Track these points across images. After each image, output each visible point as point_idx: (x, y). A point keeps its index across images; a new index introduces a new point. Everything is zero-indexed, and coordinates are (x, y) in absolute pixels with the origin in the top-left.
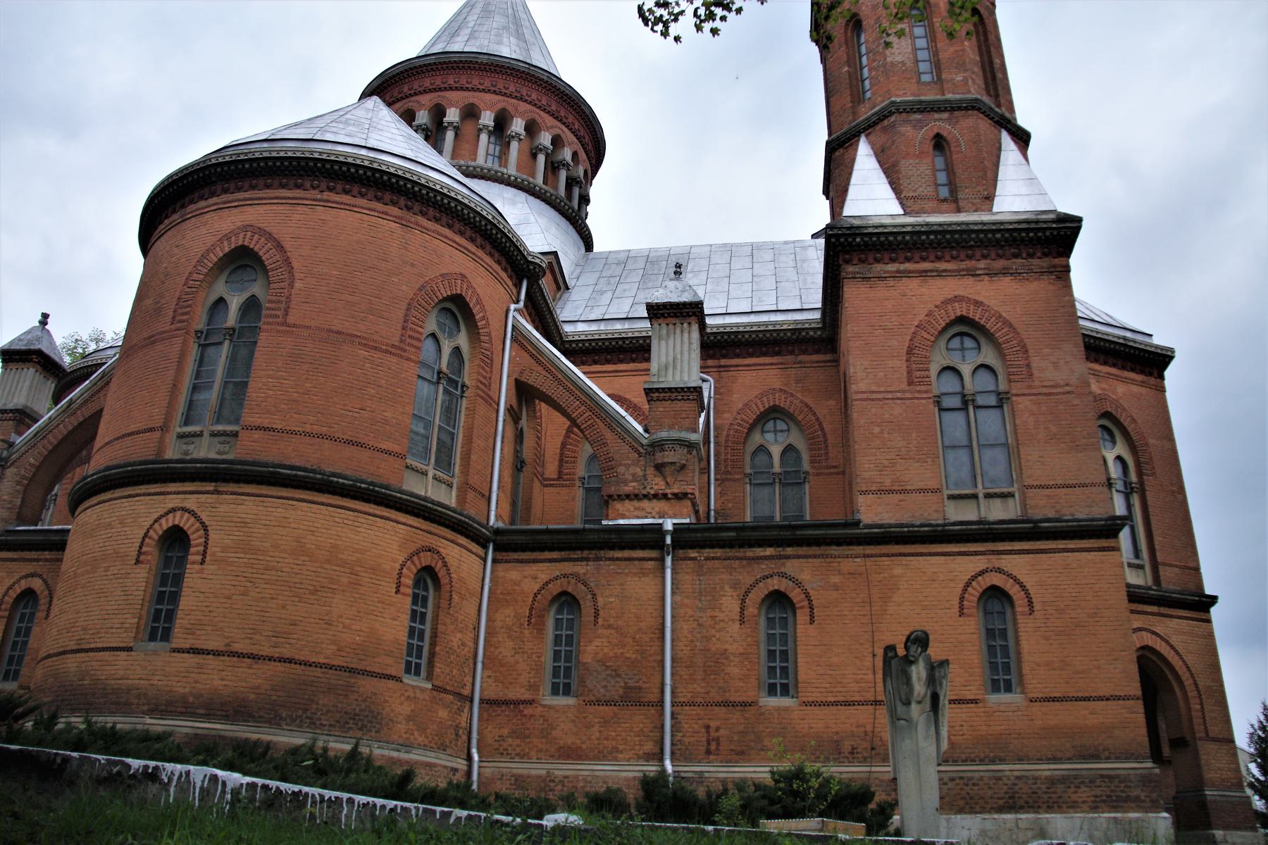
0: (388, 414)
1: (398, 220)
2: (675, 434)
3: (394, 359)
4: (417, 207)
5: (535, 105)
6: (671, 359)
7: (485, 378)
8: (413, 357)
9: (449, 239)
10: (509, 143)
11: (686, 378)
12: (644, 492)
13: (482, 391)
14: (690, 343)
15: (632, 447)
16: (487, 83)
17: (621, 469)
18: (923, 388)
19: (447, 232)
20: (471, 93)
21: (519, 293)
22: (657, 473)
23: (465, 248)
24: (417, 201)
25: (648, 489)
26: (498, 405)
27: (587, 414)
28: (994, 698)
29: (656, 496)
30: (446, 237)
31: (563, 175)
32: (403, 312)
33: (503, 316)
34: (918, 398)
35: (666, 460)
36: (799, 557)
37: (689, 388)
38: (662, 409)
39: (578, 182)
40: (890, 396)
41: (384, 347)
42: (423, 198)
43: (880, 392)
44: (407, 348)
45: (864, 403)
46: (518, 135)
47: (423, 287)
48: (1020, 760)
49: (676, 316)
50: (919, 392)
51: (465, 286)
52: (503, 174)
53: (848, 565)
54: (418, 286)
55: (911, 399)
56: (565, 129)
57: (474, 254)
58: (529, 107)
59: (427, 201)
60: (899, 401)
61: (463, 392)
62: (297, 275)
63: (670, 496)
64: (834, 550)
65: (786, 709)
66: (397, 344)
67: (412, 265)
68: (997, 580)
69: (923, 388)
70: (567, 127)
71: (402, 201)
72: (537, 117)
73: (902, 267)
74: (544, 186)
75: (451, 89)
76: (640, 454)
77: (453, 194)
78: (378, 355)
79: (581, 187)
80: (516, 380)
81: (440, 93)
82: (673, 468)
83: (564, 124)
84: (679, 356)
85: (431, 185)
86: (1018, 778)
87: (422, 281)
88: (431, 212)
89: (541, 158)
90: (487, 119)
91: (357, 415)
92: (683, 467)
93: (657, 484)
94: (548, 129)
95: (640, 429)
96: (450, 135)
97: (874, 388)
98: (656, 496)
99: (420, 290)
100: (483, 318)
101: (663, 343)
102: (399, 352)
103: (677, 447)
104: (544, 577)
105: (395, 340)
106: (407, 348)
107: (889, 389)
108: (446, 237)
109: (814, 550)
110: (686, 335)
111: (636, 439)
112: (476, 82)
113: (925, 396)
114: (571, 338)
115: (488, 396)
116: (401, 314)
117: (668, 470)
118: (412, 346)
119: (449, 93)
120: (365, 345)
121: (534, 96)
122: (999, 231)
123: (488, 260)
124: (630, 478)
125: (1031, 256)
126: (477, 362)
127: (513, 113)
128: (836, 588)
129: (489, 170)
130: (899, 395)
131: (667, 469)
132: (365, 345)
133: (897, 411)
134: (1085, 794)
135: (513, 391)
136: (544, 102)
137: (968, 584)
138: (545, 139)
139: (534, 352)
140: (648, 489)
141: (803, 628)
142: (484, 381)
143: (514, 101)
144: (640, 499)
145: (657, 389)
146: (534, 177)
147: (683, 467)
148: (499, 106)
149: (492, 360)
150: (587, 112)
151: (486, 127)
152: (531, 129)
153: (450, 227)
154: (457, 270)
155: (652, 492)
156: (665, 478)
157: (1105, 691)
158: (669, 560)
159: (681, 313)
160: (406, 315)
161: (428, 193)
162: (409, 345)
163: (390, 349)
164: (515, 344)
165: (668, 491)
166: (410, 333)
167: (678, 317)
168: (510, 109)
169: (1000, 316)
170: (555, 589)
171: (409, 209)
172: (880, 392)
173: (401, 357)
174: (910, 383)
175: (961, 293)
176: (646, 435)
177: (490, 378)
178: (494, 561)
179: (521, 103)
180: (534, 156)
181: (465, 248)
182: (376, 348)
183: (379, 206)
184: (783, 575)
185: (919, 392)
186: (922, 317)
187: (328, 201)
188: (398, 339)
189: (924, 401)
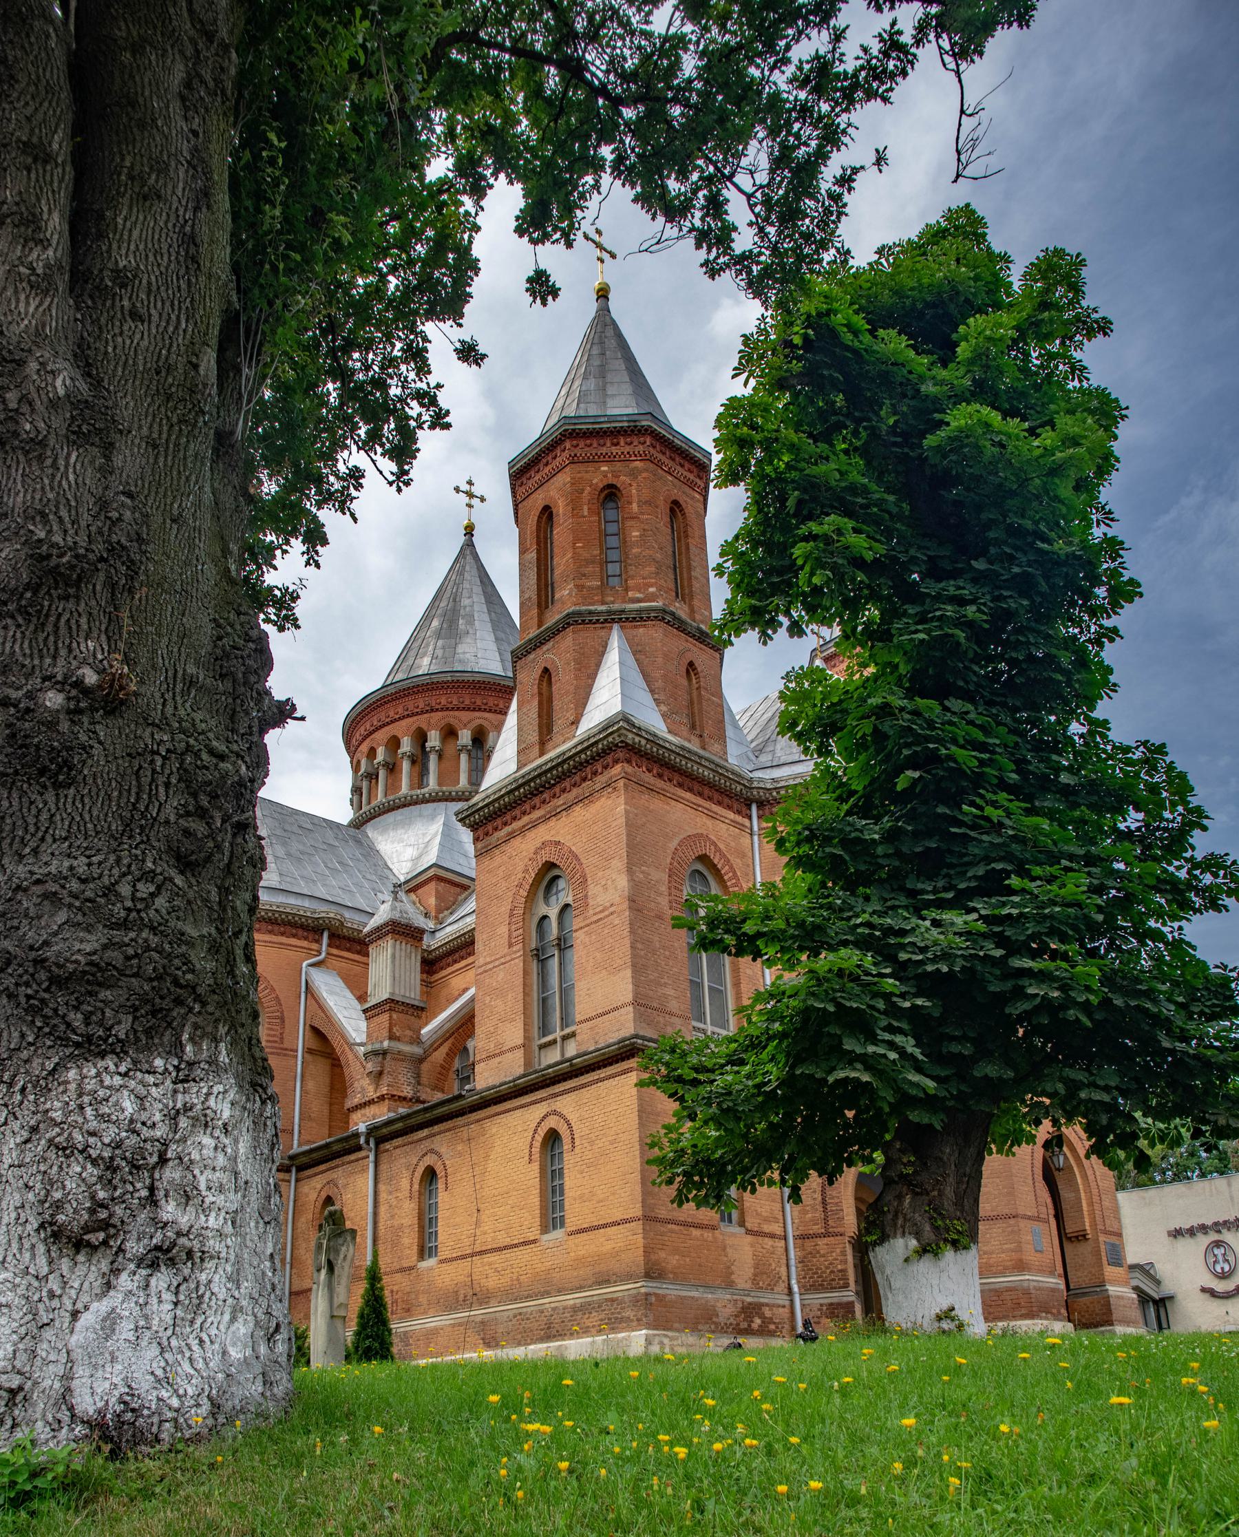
28: (546, 1237)
36: (440, 1133)
48: (560, 1291)
53: (464, 1132)
56: (487, 715)
64: (460, 1121)
65: (431, 1269)
68: (552, 1122)
72: (453, 721)
73: (508, 829)
86: (554, 1309)
89: (464, 758)
90: (406, 746)
92: (381, 1073)
93: (371, 1093)
96: (382, 773)
104: (319, 1186)
109: (450, 1124)
121: (443, 701)
122: (564, 761)
125: (595, 773)
128: (460, 1154)
133: (501, 975)
134: (595, 1318)
135: (309, 1033)
137: (535, 1131)
138: (465, 737)
141: (442, 1197)
147: (381, 1073)
148: (414, 728)
152: (450, 733)
157: (618, 1216)
158: (372, 1157)
169: (571, 851)
170: (324, 1195)
174: (510, 945)
175: (548, 838)
178: (297, 1180)
184: (432, 1151)
186: (520, 875)
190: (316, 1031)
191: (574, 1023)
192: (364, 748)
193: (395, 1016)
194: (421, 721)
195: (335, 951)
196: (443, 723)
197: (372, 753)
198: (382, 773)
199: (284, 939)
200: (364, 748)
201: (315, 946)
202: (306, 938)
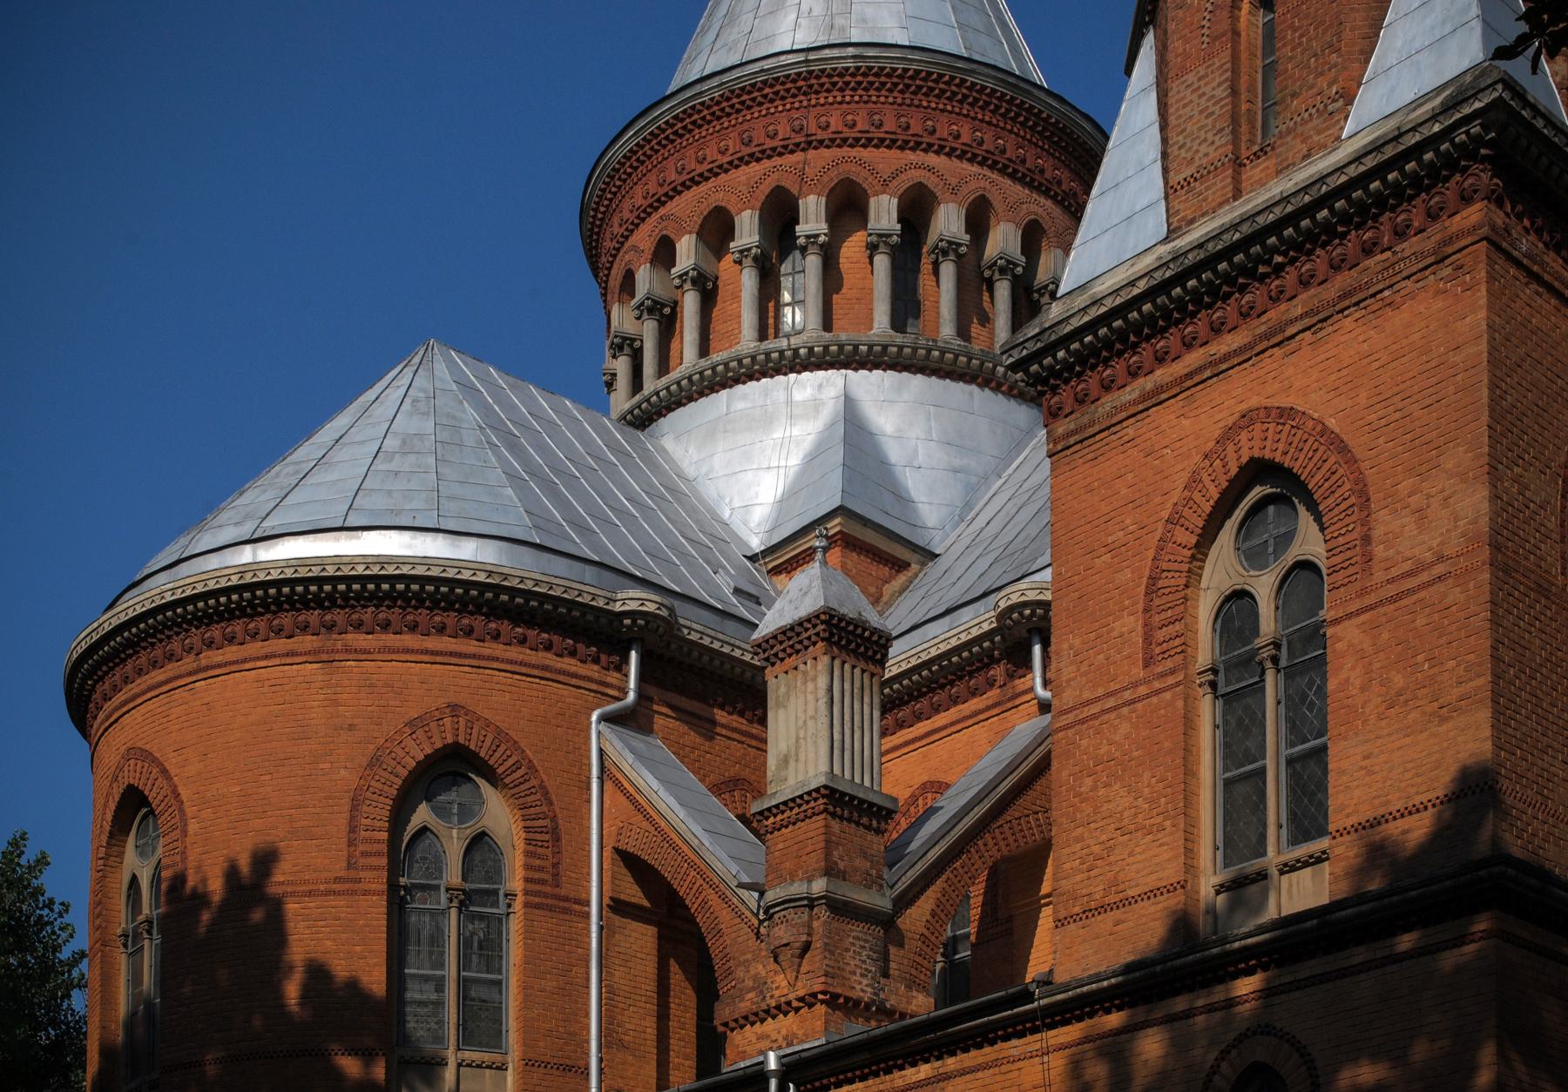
1: (314, 656)
7: (541, 869)
18: (1169, 664)
19: (408, 640)
26: (588, 903)
34: (1158, 692)
40: (1111, 703)
43: (1098, 699)
45: (1070, 732)
50: (1163, 675)
55: (1148, 696)
57: (474, 656)
60: (1125, 710)
67: (351, 727)
69: (1169, 664)
80: (617, 850)
90: (748, 231)
97: (1087, 695)
99: (370, 765)
100: (517, 766)
107: (1113, 687)
113: (1171, 680)
115: (557, 897)
130: (1127, 695)
142: (537, 875)
151: (744, 252)
154: (441, 702)
171: (330, 627)
172: (1098, 699)
177: (555, 865)
181: (451, 654)
185: (1163, 675)
189: (1168, 695)
190: (631, 862)
191: (1322, 832)
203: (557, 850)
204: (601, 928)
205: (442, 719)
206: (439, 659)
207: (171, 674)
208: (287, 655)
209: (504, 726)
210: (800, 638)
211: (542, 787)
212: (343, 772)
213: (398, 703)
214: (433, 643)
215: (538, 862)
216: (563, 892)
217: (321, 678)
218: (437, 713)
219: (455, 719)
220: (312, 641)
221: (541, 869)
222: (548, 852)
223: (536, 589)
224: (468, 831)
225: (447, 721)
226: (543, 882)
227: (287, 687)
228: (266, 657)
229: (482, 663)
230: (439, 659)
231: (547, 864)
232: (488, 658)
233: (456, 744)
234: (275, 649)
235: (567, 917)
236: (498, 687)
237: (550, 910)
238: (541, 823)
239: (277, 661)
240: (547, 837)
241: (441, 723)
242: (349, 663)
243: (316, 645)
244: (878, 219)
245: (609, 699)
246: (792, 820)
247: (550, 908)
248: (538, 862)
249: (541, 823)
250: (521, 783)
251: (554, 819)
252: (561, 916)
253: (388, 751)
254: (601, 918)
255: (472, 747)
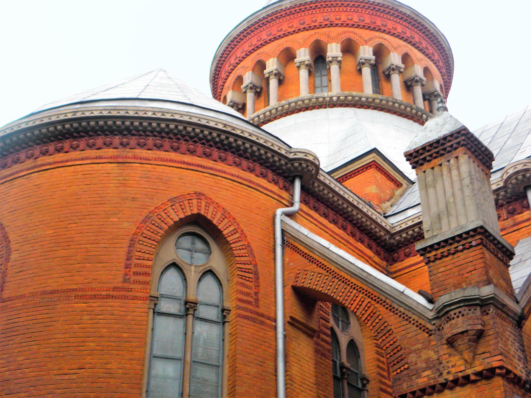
0: (113, 366)
2: (458, 295)
3: (116, 303)
4: (133, 141)
5: (348, 25)
6: (442, 206)
7: (248, 294)
8: (140, 294)
9: (175, 162)
10: (329, 68)
11: (463, 221)
12: (441, 380)
13: (246, 310)
14: (461, 180)
15: (421, 327)
16: (296, 24)
17: (412, 358)
19: (173, 155)
20: (283, 40)
21: (292, 195)
22: (451, 351)
23: (198, 166)
24: (134, 135)
25: (445, 376)
26: (275, 320)
27: (366, 302)
29: (456, 383)
30: (173, 161)
31: (396, 79)
32: (126, 250)
33: (270, 224)
35: (455, 331)
37: (467, 233)
38: (443, 269)
39: (417, 81)
41: (104, 293)
42: (138, 131)
44: (132, 286)
46: (335, 58)
47: (147, 218)
49: (439, 155)
51: (203, 204)
52: (324, 98)
54: (141, 219)
57: (211, 169)
58: (340, 29)
59: (144, 132)
61: (224, 317)
62: (13, 246)
63: (473, 377)
66: (120, 285)
67: (133, 199)
70: (389, 33)
71: (117, 140)
72: (352, 36)
74: (375, 96)
75: (266, 43)
76: (430, 333)
77: (168, 116)
78: (95, 304)
79: (423, 85)
81: (258, 51)
82: (466, 338)
83: (384, 31)
84: (451, 200)
85: (141, 114)
87: (145, 213)
88: (150, 141)
89: (367, 71)
91: (74, 377)
92: (480, 335)
94: (366, 42)
95: (422, 301)
96: (273, 83)
98: (456, 383)
99: (144, 221)
100: (235, 232)
101: (431, 191)
102: (122, 293)
103: (465, 310)
105: (118, 281)
106: (132, 286)
108: (173, 161)
110: (455, 172)
111: (421, 316)
112: (285, 27)
114: (398, 229)
116: (122, 253)
117: (462, 343)
118: (140, 282)
119: (265, 47)
120: (82, 297)
121: (344, 17)
123: (234, 170)
124: (424, 365)
126: (236, 279)
127: (326, 41)
129: (310, 100)
131: (459, 342)
132: (82, 297)
135: (292, 299)
136: (356, 19)
139: (306, 251)
140: (445, 376)
142: (245, 298)
143: (324, 30)
144: (440, 392)
145: (432, 246)
146: (362, 90)
147: (480, 335)
148: (312, 40)
149: (256, 273)
150: (408, 13)
151: (302, 63)
153: (175, 150)
154: (191, 190)
155: (451, 378)
156: (461, 354)
159: (444, 149)
160: (129, 252)
161: (141, 124)
162: (135, 282)
163: (111, 293)
164: (287, 249)
165: (469, 372)
166: (134, 269)
167: (442, 155)
168: (323, 39)
171: (124, 145)
173: (126, 297)
176: (430, 306)
177: (256, 294)
179: (332, 29)
180: (360, 71)
181: (198, 166)
182: (95, 297)
183: (93, 153)
187: (42, 165)
188: (121, 279)
192: (250, 61)
193: (488, 255)
194: (320, 34)
195: (305, 208)
196: (344, 37)
197: (261, 65)
198: (273, 83)
199: (252, 177)
200: (250, 61)
201: (285, 195)
202: (276, 183)
203: (257, 285)
204: (285, 336)
205: (191, 199)
206: (191, 167)
207: (14, 170)
208: (96, 158)
209: (228, 209)
210: (445, 147)
211: (249, 246)
212: (125, 224)
213: (163, 188)
214: (188, 158)
215: (246, 290)
216: (261, 310)
217: (116, 171)
218: (188, 196)
219: (199, 201)
220: (113, 152)
221: (248, 294)
222: (252, 284)
223: (250, 137)
224: (201, 268)
225: (195, 202)
226: (249, 303)
227: (93, 176)
228: (82, 159)
229: (217, 173)
230: (191, 167)
231: (252, 292)
232: (220, 171)
233: (199, 215)
234: (89, 155)
235: (263, 327)
236: (224, 187)
237: (254, 321)
238: (247, 266)
239: (89, 161)
240: (251, 276)
241: (190, 201)
242: (135, 165)
243: (115, 154)
244: (364, 53)
245: (283, 205)
246: (452, 252)
247: (254, 320)
248: (246, 290)
249: (247, 266)
250: (237, 242)
251: (256, 265)
252: (260, 326)
253: (156, 214)
254: (285, 330)
255: (209, 217)
